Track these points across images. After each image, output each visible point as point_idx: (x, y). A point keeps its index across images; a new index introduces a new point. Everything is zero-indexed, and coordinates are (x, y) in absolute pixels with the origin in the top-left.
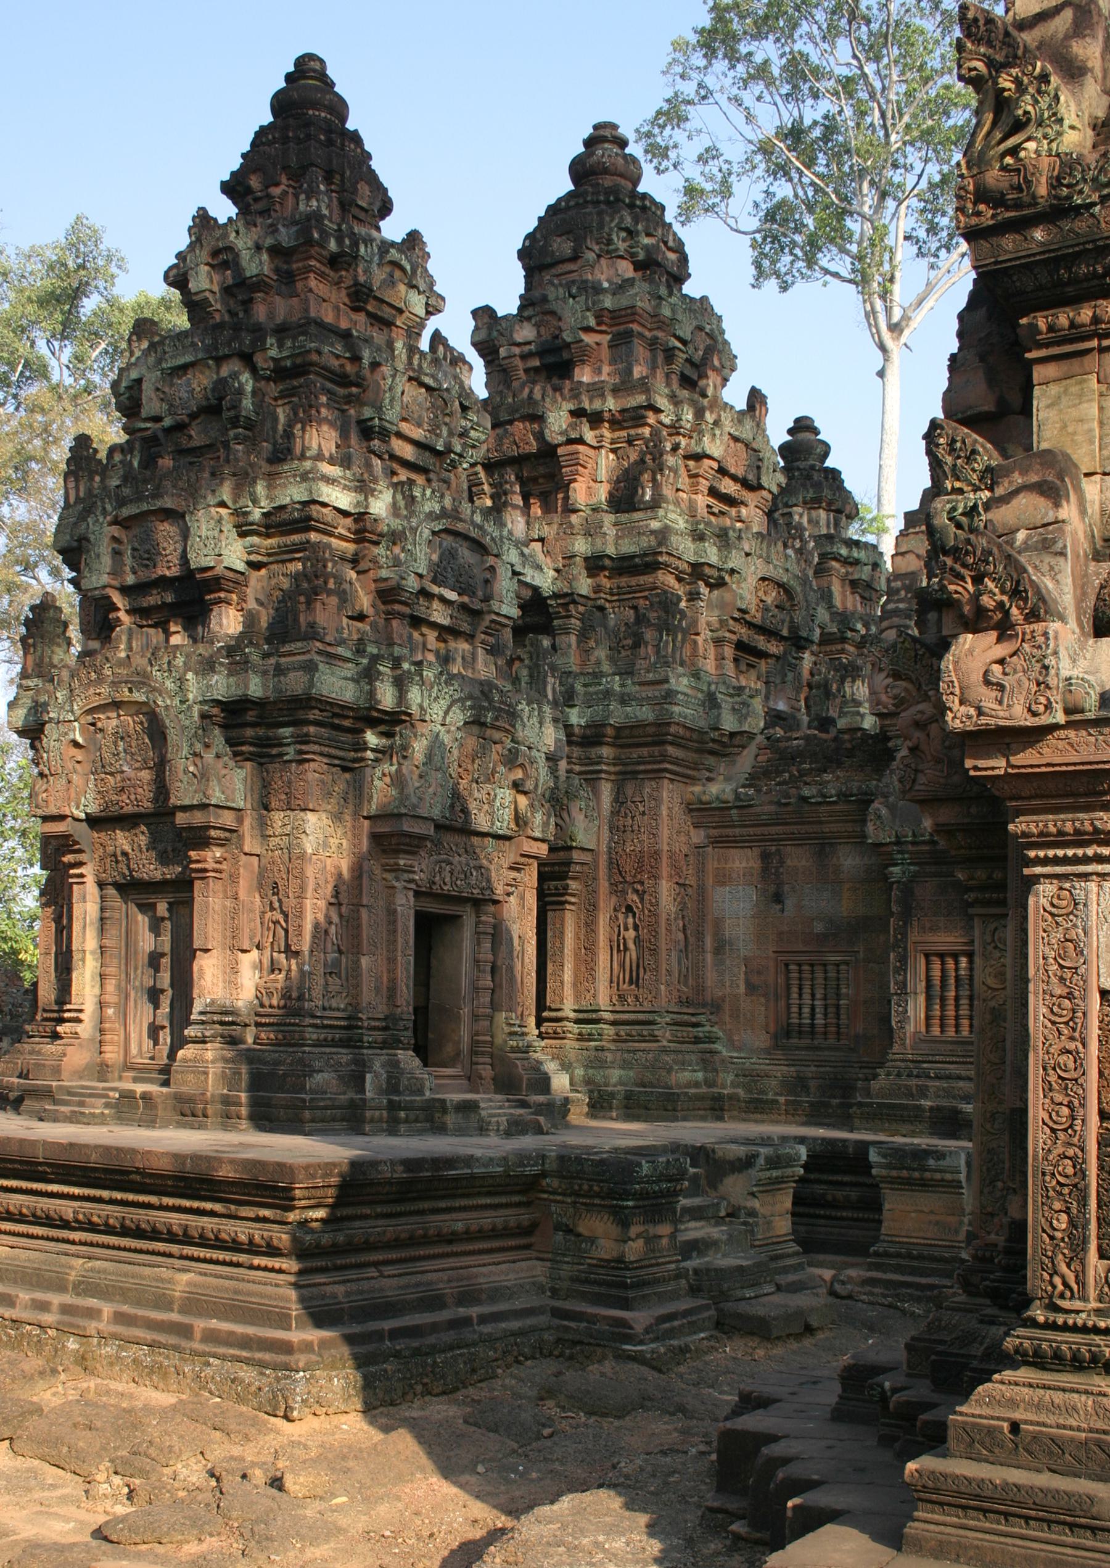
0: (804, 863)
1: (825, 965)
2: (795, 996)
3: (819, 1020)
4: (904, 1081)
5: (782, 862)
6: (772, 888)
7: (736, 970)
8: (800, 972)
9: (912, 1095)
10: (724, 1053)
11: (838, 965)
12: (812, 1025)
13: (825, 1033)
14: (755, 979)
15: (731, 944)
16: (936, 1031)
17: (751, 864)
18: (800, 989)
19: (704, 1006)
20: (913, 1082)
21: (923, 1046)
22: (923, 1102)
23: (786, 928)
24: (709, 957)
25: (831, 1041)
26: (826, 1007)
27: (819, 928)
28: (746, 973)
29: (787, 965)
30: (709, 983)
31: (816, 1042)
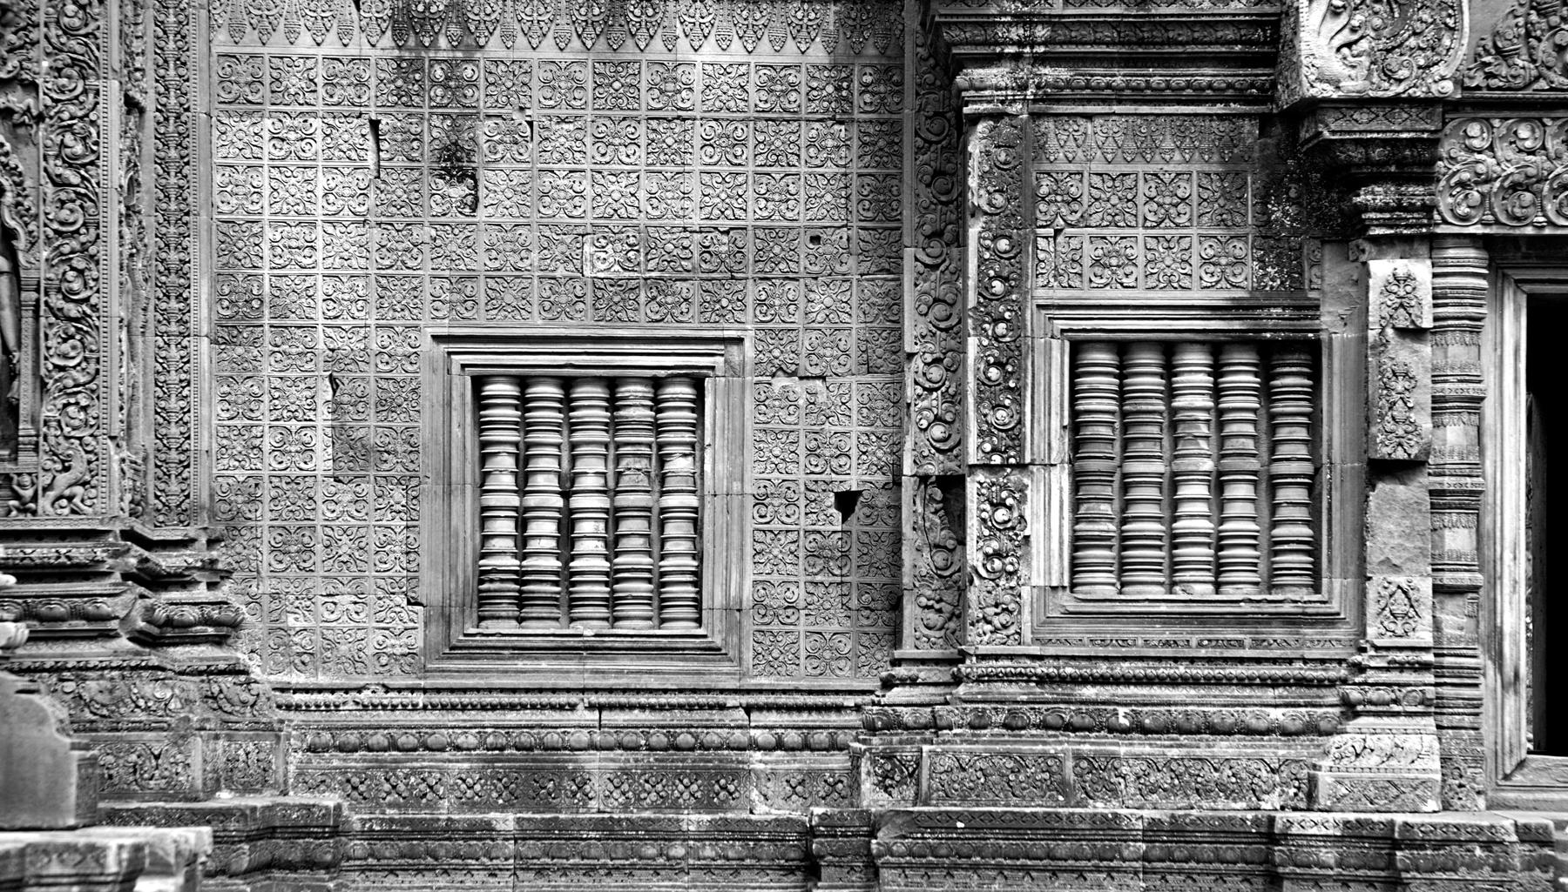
0: (548, 50)
1: (612, 384)
2: (508, 481)
3: (590, 557)
4: (1033, 744)
5: (469, 45)
6: (435, 131)
7: (298, 395)
8: (523, 404)
9: (1063, 787)
10: (256, 673)
11: (657, 384)
12: (567, 577)
13: (612, 602)
14: (370, 428)
15: (280, 312)
16: (1101, 585)
17: (358, 46)
18: (523, 460)
19: (185, 515)
20: (1064, 746)
21: (1074, 630)
22: (1100, 807)
23: (481, 262)
24: (203, 349)
25: (635, 625)
26: (614, 517)
27: (601, 263)
28: (337, 407)
29: (479, 382)
30: (204, 441)
31: (587, 630)
